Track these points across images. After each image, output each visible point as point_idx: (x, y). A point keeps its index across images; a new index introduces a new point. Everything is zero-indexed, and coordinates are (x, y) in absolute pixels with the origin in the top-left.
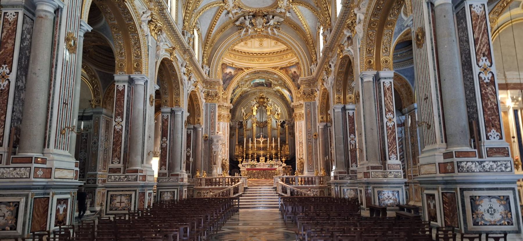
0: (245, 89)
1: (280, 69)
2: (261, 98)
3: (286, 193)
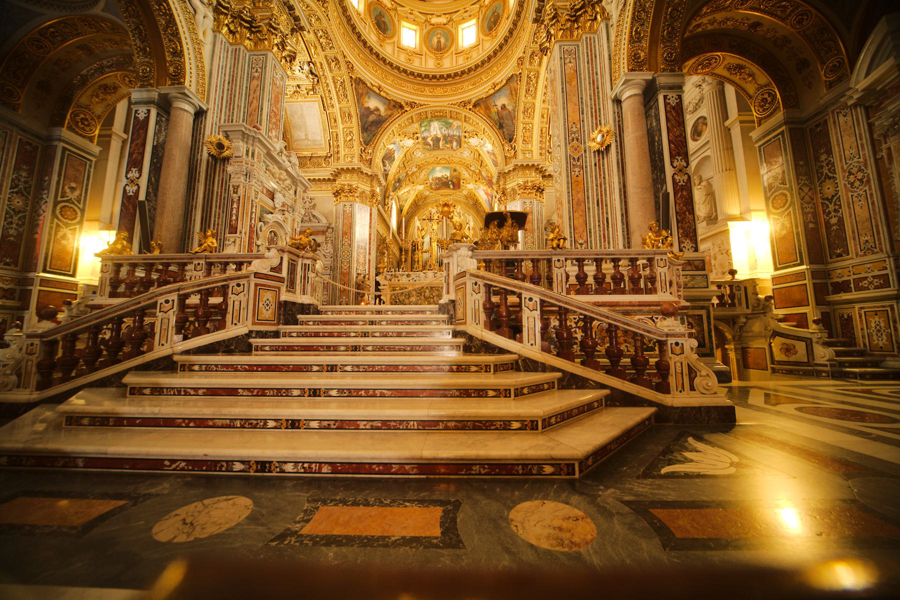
0: (421, 187)
1: (475, 106)
2: (446, 205)
3: (515, 331)
